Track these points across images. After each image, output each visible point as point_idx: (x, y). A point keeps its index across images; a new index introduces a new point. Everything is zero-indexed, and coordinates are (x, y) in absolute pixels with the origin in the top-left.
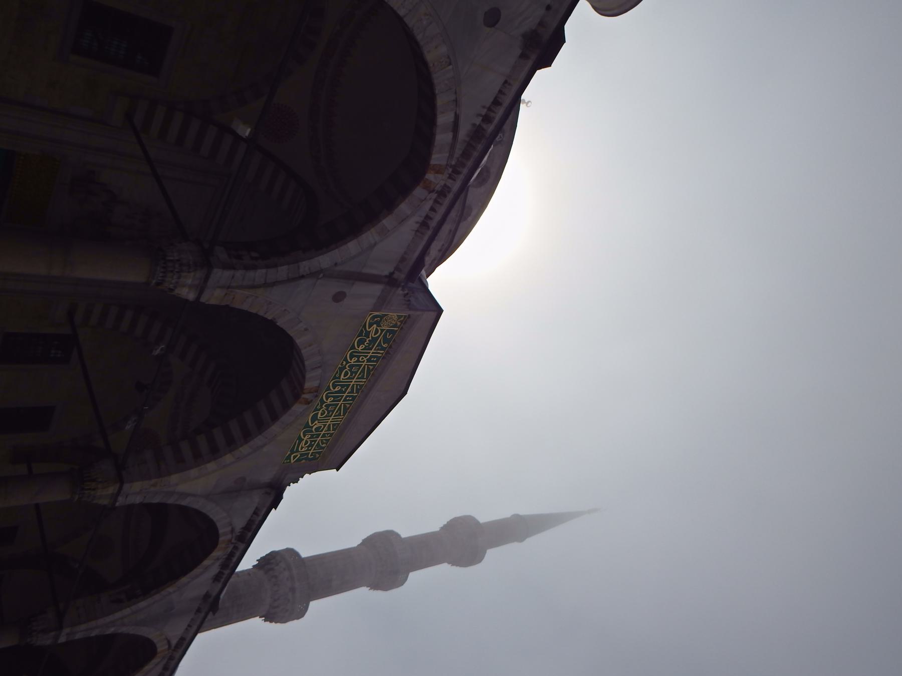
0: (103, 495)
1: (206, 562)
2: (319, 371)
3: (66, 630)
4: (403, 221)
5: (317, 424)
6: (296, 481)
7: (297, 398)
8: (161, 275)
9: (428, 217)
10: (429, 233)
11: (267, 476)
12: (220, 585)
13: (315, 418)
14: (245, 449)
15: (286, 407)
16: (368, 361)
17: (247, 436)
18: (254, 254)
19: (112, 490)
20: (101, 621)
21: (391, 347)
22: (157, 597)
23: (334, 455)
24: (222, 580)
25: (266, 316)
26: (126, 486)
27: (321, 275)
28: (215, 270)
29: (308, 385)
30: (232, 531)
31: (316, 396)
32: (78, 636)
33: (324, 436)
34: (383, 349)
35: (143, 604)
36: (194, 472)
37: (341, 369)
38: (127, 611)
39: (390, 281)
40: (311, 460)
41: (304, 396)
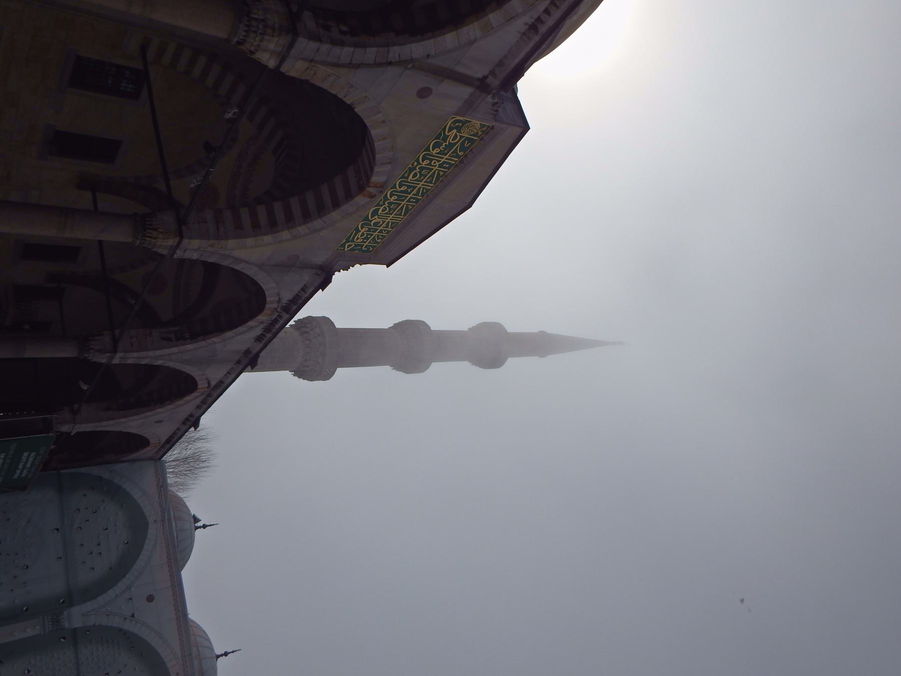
0: (163, 244)
2: (389, 167)
3: (119, 355)
4: (510, 19)
6: (346, 269)
7: (361, 189)
8: (244, 33)
9: (539, 20)
10: (537, 38)
11: (320, 259)
12: (260, 345)
14: (302, 229)
15: (349, 196)
16: (440, 166)
17: (307, 217)
18: (344, 28)
19: (171, 242)
20: (151, 353)
21: (466, 156)
22: (203, 343)
23: (388, 251)
24: (264, 342)
25: (345, 99)
26: (185, 242)
27: (410, 66)
29: (374, 179)
30: (279, 301)
31: (381, 192)
32: (129, 361)
33: (381, 231)
34: (458, 156)
35: (189, 347)
36: (250, 241)
37: (411, 170)
38: (175, 350)
39: (482, 85)
40: (364, 251)
41: (368, 189)
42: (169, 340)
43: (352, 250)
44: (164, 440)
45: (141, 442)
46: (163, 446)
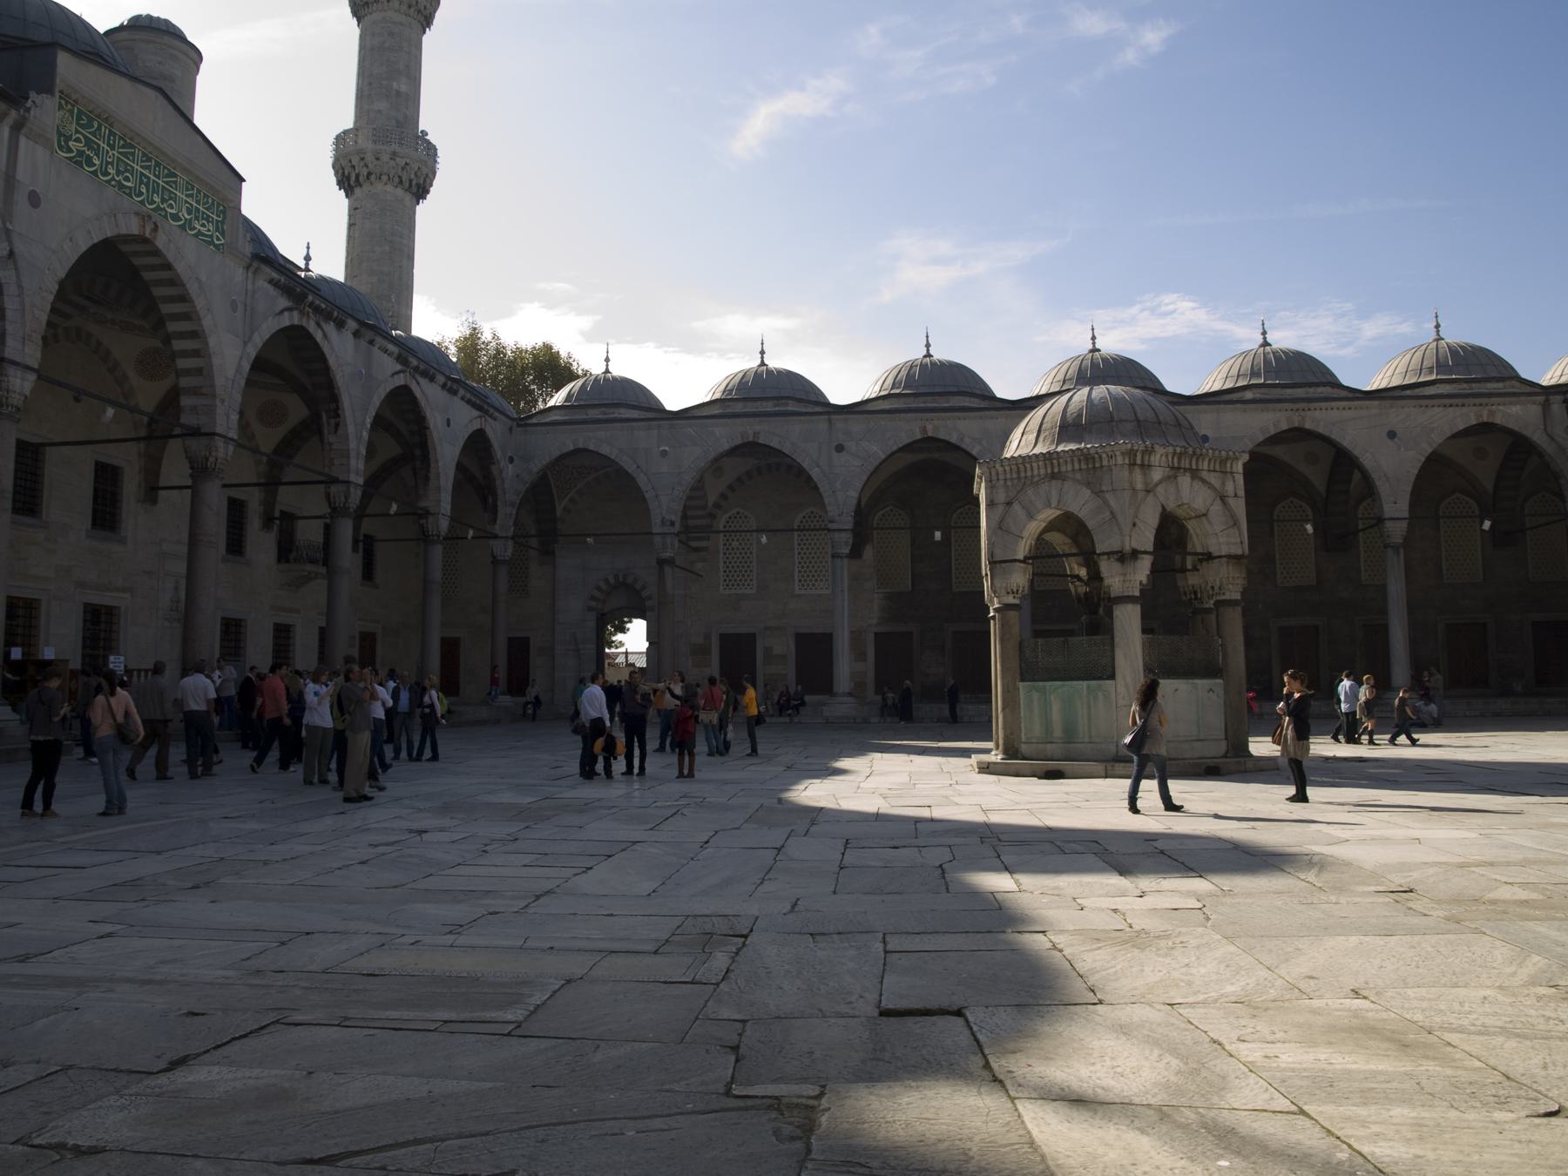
1: (319, 336)
3: (353, 478)
5: (184, 215)
13: (176, 217)
14: (200, 303)
15: (157, 253)
16: (113, 148)
17: (184, 298)
19: (220, 443)
20: (353, 445)
26: (219, 430)
28: (6, 355)
30: (289, 309)
32: (361, 466)
33: (198, 202)
34: (99, 128)
36: (216, 361)
42: (337, 425)
43: (223, 234)
44: (476, 413)
45: (477, 444)
46: (486, 412)
